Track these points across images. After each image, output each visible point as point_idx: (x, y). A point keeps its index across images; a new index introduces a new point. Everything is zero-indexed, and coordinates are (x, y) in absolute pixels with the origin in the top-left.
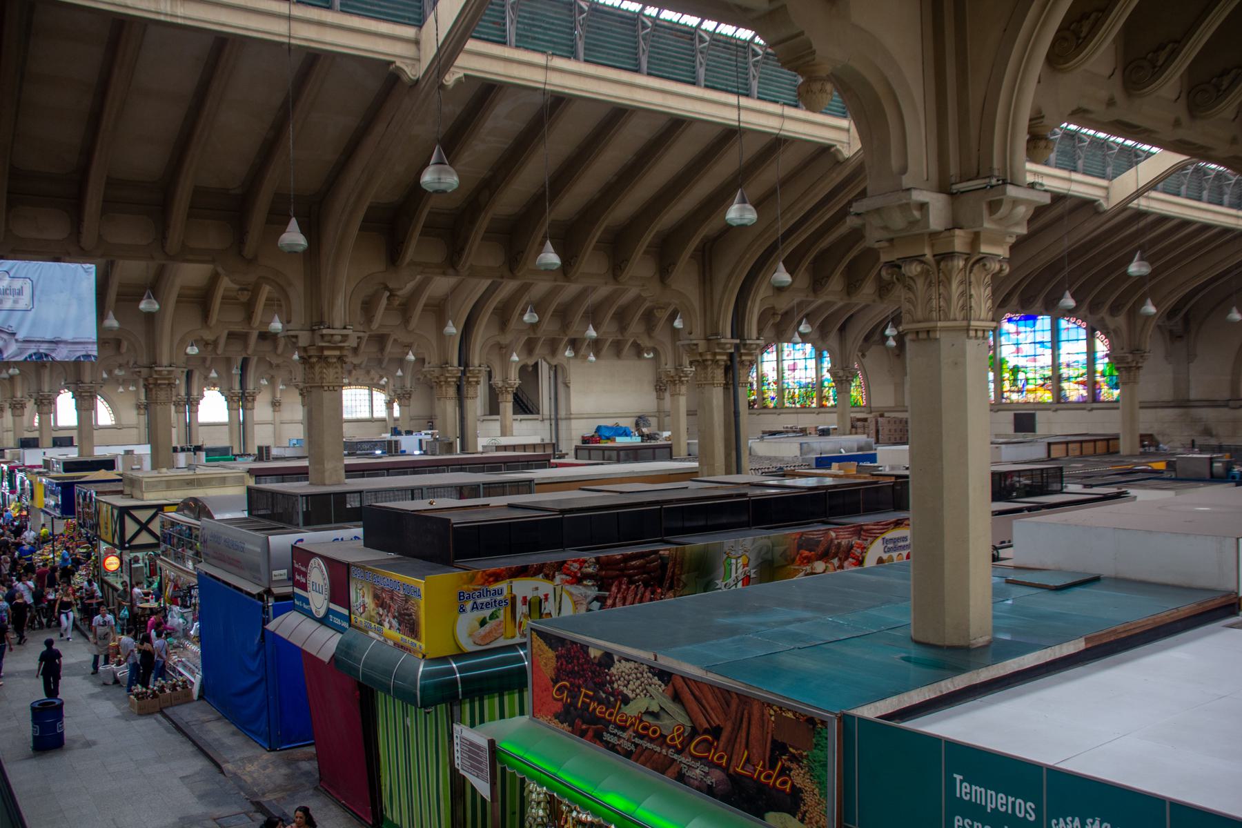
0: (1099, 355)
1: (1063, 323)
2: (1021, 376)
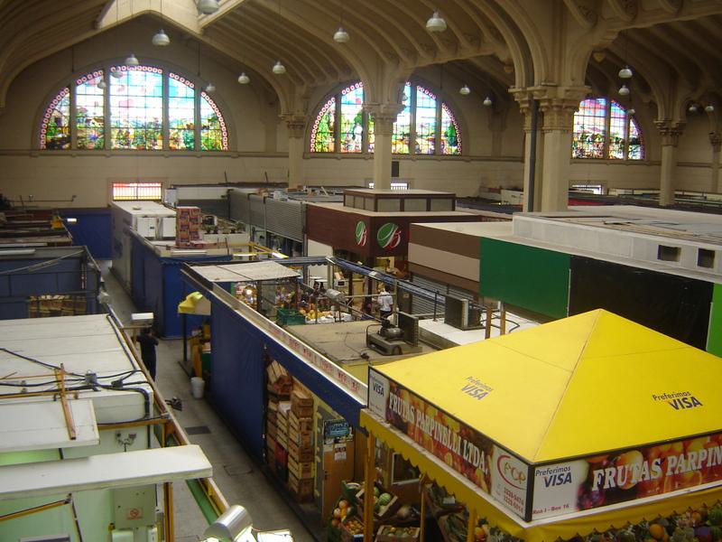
0: (443, 120)
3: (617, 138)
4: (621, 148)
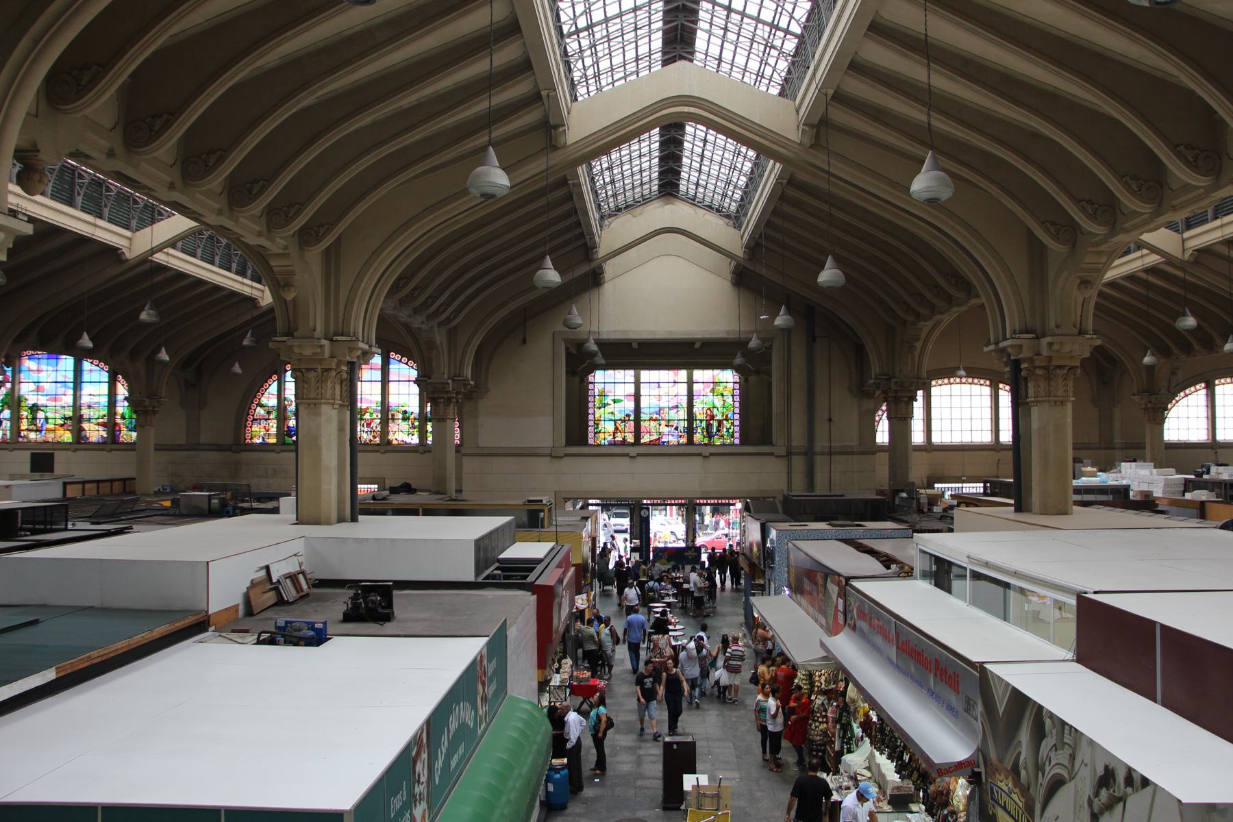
0: (120, 397)
1: (87, 365)
2: (41, 415)
3: (405, 412)
4: (413, 427)
